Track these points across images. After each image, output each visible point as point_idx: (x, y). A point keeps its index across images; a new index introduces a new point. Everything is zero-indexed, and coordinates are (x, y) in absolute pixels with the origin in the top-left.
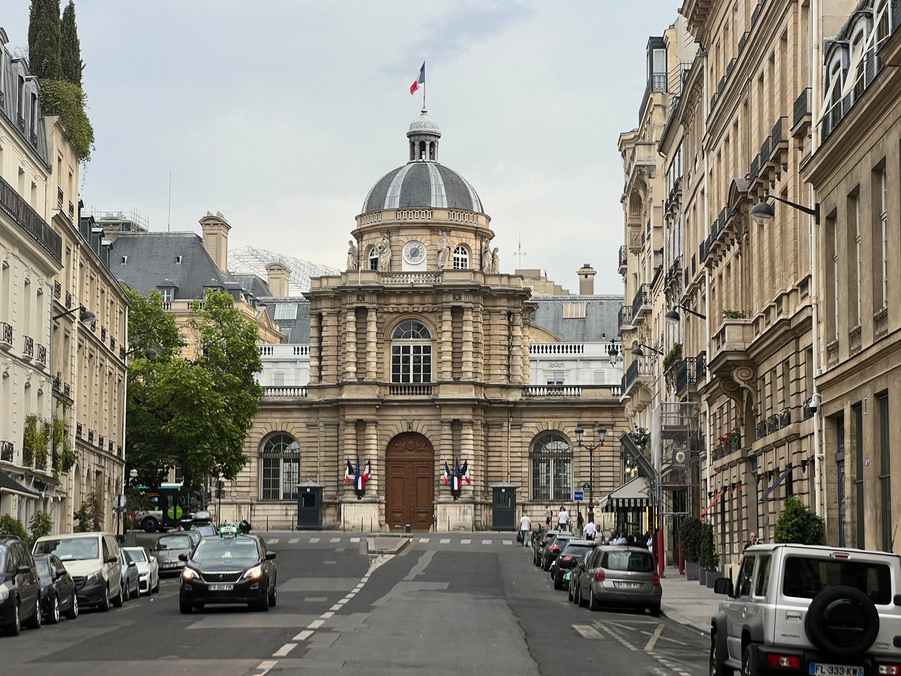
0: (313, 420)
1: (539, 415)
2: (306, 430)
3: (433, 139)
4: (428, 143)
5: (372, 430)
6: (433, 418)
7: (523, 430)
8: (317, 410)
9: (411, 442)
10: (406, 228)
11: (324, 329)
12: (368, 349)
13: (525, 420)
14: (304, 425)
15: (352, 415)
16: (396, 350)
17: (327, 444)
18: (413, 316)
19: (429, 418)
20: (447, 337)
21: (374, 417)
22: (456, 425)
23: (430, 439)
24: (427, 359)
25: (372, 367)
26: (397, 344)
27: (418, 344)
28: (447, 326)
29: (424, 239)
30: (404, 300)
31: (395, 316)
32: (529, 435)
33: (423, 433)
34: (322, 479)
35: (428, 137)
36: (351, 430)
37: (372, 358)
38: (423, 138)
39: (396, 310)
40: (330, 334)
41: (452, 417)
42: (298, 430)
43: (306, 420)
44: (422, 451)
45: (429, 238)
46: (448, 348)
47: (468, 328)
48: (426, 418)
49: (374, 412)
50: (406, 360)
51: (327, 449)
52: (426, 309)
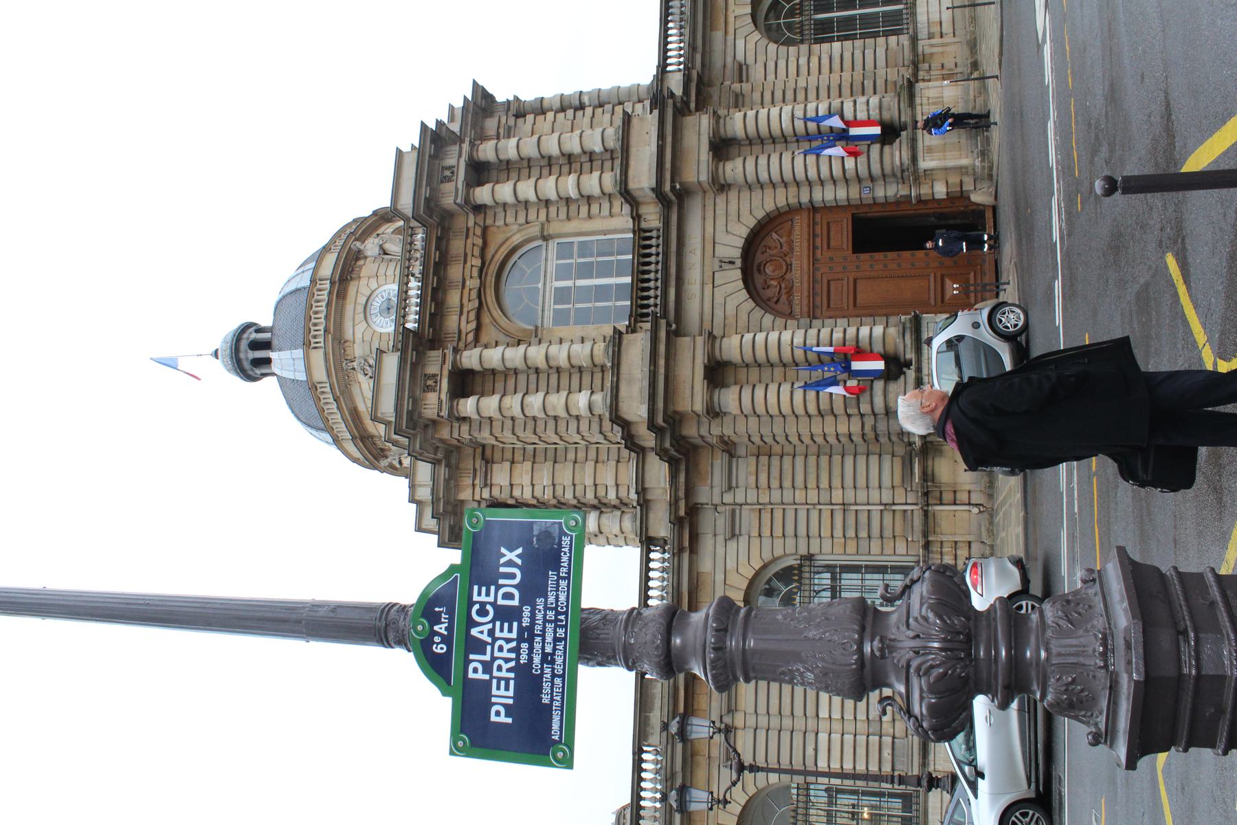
0: (721, 522)
1: (718, 35)
2: (743, 541)
4: (254, 336)
5: (731, 348)
6: (710, 214)
7: (750, 61)
8: (694, 510)
9: (769, 270)
11: (517, 493)
12: (541, 362)
13: (729, 60)
14: (732, 545)
15: (692, 392)
16: (561, 318)
17: (775, 483)
18: (491, 280)
19: (709, 222)
21: (700, 340)
22: (722, 147)
23: (760, 214)
24: (584, 249)
25: (581, 353)
26: (549, 314)
27: (551, 268)
30: (453, 298)
31: (486, 319)
32: (761, 50)
33: (744, 232)
34: (862, 496)
35: (245, 336)
36: (729, 398)
37: (560, 355)
38: (244, 345)
39: (472, 316)
40: (526, 480)
41: (705, 154)
42: (743, 558)
43: (720, 539)
44: (790, 244)
45: (363, 282)
48: (709, 229)
49: (685, 342)
50: (585, 294)
51: (787, 483)
52: (477, 251)
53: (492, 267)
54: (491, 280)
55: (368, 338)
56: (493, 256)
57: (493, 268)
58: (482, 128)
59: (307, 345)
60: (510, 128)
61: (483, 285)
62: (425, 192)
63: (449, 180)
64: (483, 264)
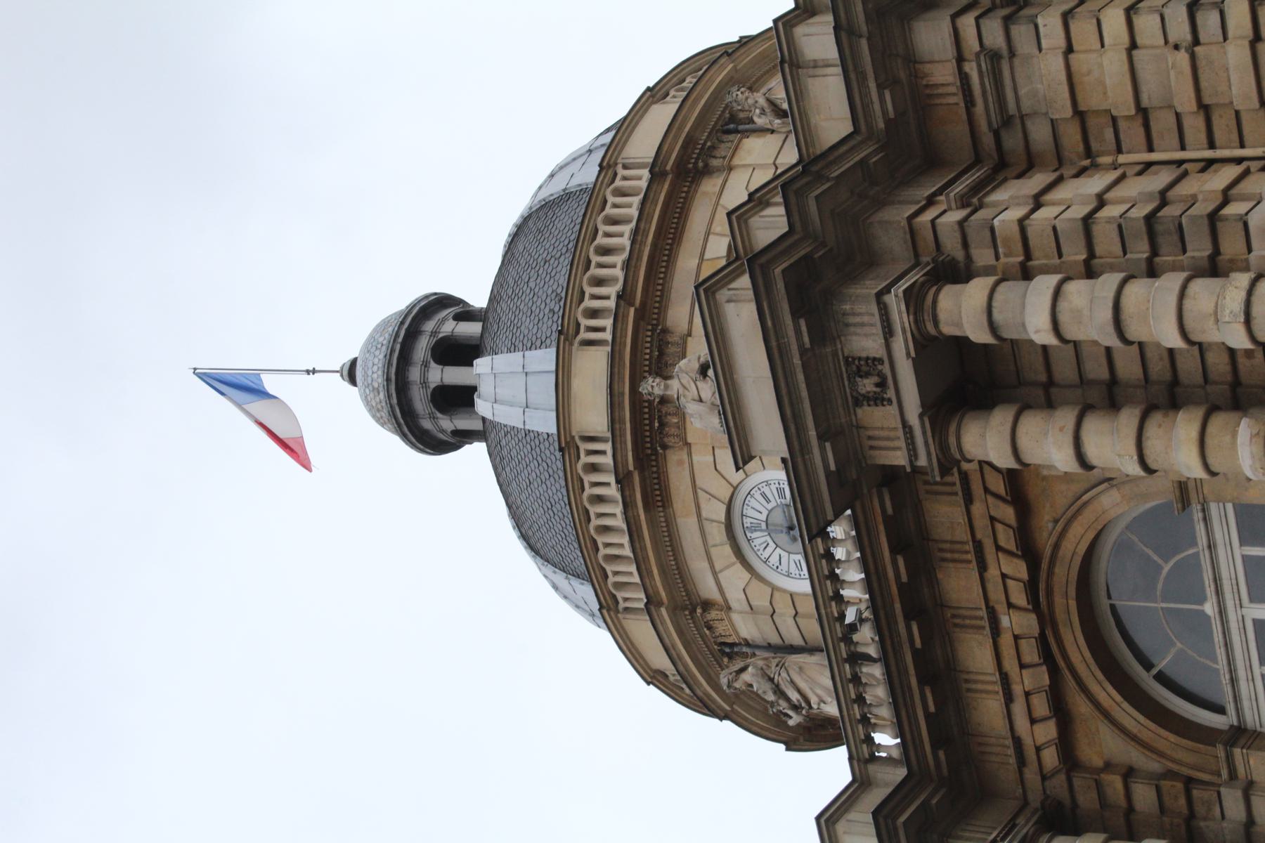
3: (423, 347)
10: (677, 572)
18: (1066, 606)
20: (1110, 443)
28: (1048, 444)
29: (707, 480)
30: (977, 654)
31: (1081, 707)
35: (414, 374)
39: (1041, 706)
46: (1178, 445)
47: (1031, 314)
52: (1007, 539)
53: (1059, 571)
54: (1066, 606)
55: (761, 601)
56: (1056, 547)
57: (1064, 576)
58: (912, 60)
59: (566, 339)
60: (995, 57)
61: (1047, 620)
62: (822, 458)
63: (878, 400)
64: (1034, 567)
